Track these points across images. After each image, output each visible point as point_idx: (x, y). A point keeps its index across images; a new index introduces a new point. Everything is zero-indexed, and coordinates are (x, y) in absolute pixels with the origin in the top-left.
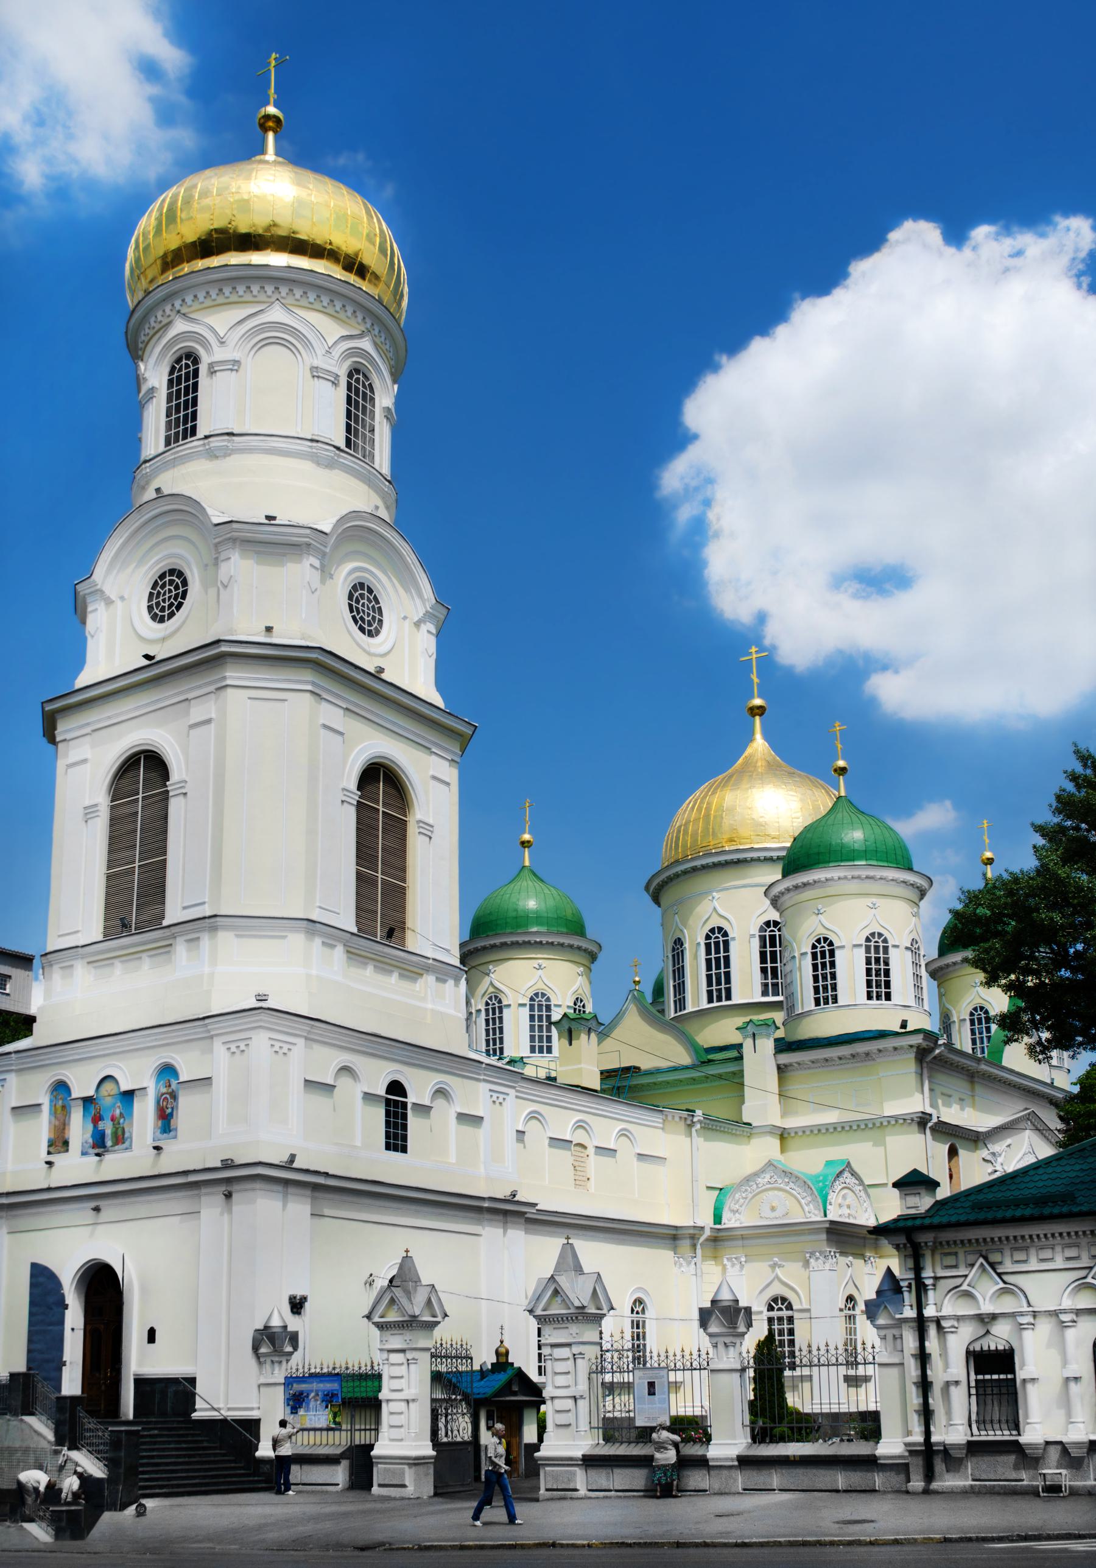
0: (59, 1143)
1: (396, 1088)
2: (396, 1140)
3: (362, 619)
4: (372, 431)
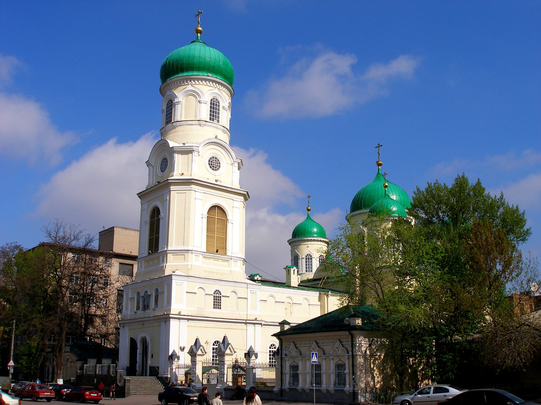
0: (138, 308)
1: (217, 292)
2: (217, 304)
3: (213, 167)
4: (219, 114)
